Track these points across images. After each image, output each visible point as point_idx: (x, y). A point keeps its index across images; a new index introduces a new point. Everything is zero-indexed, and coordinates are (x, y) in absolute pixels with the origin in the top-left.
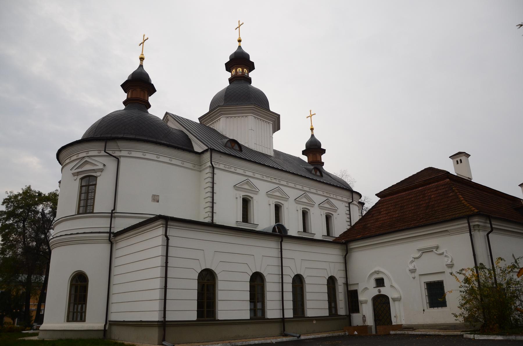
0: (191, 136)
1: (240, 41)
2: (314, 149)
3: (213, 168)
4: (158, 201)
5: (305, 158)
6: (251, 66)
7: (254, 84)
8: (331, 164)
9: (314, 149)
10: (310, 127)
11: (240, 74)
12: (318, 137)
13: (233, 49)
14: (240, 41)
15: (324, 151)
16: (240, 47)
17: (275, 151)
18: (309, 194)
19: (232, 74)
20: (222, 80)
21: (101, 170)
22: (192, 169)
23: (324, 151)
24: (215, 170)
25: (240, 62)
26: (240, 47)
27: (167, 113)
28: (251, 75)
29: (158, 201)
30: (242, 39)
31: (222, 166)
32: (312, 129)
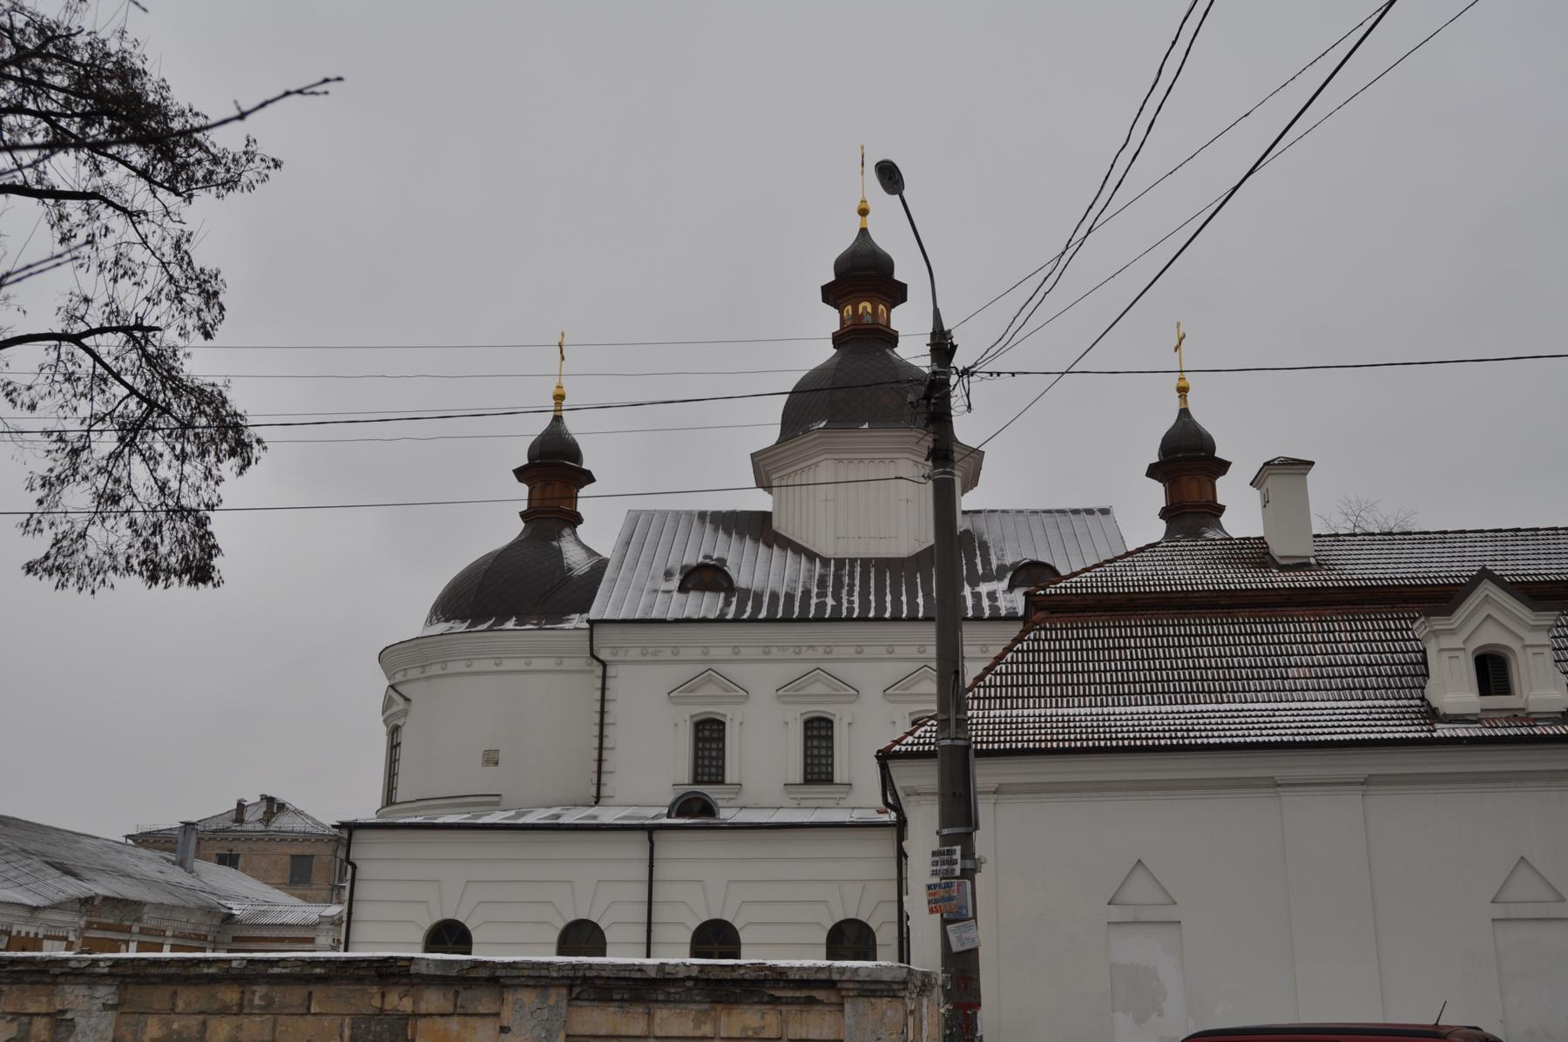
1: (863, 212)
3: (604, 664)
4: (496, 764)
14: (863, 212)
16: (864, 232)
21: (405, 713)
22: (582, 672)
24: (611, 671)
26: (864, 232)
29: (496, 764)
31: (634, 654)
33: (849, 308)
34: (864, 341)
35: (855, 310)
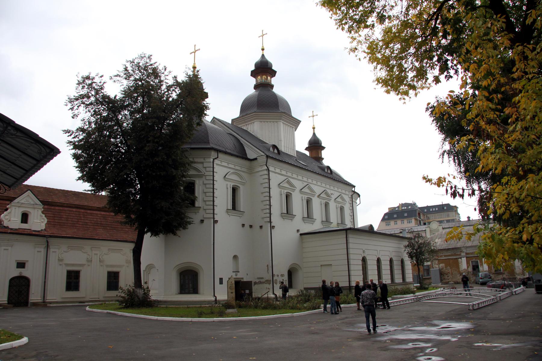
0: (243, 141)
1: (263, 50)
2: (315, 145)
5: (307, 153)
6: (273, 73)
7: (275, 90)
8: (328, 158)
9: (315, 145)
10: (312, 126)
12: (319, 136)
13: (258, 58)
14: (263, 50)
15: (324, 148)
16: (263, 55)
17: (297, 152)
18: (311, 185)
19: (257, 80)
23: (324, 148)
25: (263, 69)
26: (263, 55)
27: (214, 118)
28: (274, 81)
32: (314, 128)
34: (264, 87)
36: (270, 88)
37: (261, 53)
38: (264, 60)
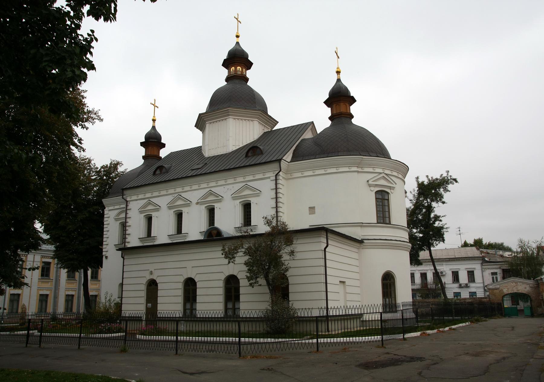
1: (238, 37)
6: (248, 65)
11: (239, 73)
13: (231, 46)
14: (238, 37)
16: (238, 43)
19: (229, 72)
20: (219, 78)
25: (237, 60)
26: (238, 43)
28: (249, 74)
30: (240, 34)
33: (233, 68)
35: (236, 69)
36: (244, 82)
37: (236, 40)
38: (238, 47)
